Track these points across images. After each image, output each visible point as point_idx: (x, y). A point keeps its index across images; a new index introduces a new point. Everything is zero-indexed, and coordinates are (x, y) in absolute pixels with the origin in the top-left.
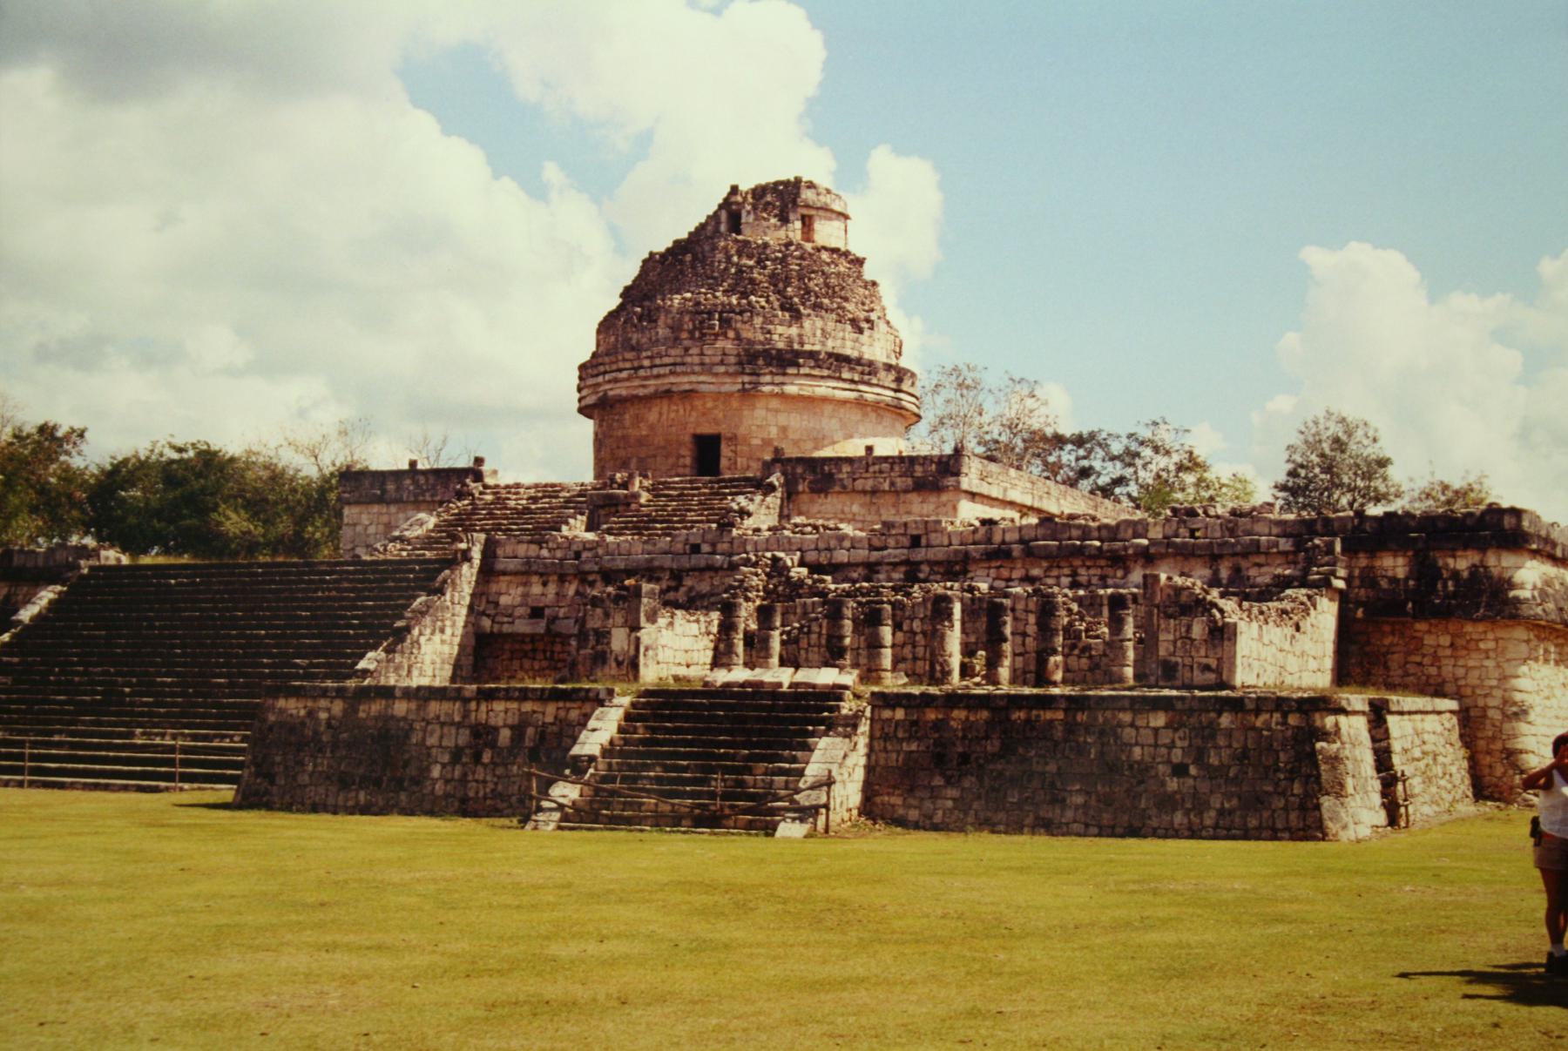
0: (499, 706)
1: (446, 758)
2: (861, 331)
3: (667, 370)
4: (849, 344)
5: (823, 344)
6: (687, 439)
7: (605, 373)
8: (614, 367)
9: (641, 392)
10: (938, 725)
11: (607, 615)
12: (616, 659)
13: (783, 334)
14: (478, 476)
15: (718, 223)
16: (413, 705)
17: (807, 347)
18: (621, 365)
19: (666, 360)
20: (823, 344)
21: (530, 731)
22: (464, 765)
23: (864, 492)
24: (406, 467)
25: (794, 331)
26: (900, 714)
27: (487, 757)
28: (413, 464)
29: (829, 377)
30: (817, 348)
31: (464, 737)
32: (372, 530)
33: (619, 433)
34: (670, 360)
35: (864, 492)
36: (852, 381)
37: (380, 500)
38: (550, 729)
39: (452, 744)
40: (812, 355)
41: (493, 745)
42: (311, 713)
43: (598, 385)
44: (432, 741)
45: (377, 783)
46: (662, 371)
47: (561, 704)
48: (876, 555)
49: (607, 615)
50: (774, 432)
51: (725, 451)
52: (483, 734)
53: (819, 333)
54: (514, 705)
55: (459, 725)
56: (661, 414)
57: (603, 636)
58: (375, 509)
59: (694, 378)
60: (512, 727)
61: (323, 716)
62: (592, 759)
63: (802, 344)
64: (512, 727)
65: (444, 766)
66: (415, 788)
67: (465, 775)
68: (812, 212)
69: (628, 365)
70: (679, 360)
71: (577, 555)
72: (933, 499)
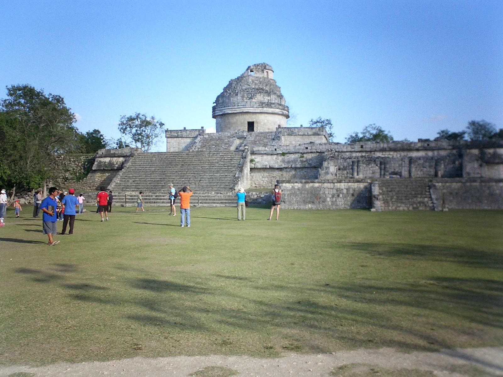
0: (342, 184)
1: (331, 196)
2: (281, 99)
4: (279, 101)
5: (275, 101)
6: (247, 123)
8: (227, 106)
9: (235, 112)
10: (450, 186)
11: (328, 163)
12: (331, 173)
13: (266, 99)
14: (203, 131)
15: (248, 73)
16: (320, 184)
17: (272, 102)
18: (229, 105)
20: (275, 101)
21: (351, 190)
22: (336, 198)
23: (301, 135)
24: (183, 129)
25: (269, 98)
26: (440, 184)
27: (341, 195)
28: (185, 128)
30: (274, 102)
31: (335, 191)
32: (175, 144)
34: (243, 104)
35: (301, 135)
37: (177, 137)
38: (356, 189)
39: (332, 193)
40: (274, 104)
41: (343, 194)
42: (293, 187)
43: (222, 110)
44: (327, 192)
45: (313, 202)
47: (358, 183)
48: (353, 150)
49: (328, 163)
50: (266, 121)
51: (255, 124)
52: (339, 190)
54: (346, 184)
55: (333, 189)
57: (327, 168)
58: (175, 139)
59: (248, 108)
60: (347, 189)
61: (296, 187)
62: (378, 195)
63: (271, 101)
64: (347, 189)
65: (330, 198)
66: (323, 203)
67: (336, 200)
70: (245, 104)
71: (276, 150)
72: (317, 137)
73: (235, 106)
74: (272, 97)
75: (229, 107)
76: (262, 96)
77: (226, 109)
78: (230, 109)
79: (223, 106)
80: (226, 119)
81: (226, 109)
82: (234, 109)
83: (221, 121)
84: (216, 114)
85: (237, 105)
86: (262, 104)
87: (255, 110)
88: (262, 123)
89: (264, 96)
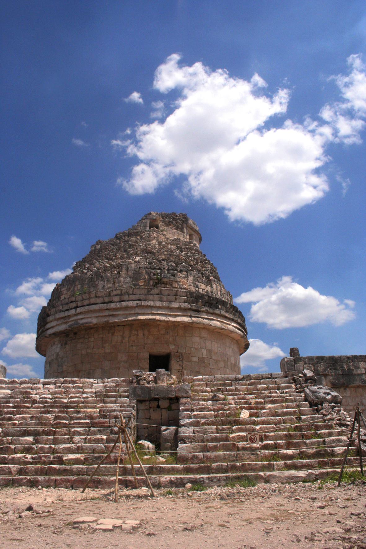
3: (135, 302)
6: (147, 355)
7: (76, 307)
8: (86, 302)
13: (203, 288)
18: (93, 300)
19: (133, 297)
25: (208, 289)
29: (232, 320)
33: (84, 352)
36: (239, 324)
43: (69, 317)
46: (131, 304)
50: (205, 352)
53: (219, 293)
56: (123, 337)
68: (193, 233)
69: (99, 300)
73: (111, 302)
74: (214, 286)
75: (92, 307)
76: (191, 278)
77: (81, 313)
78: (95, 311)
79: (74, 305)
80: (79, 346)
81: (81, 313)
82: (107, 313)
83: (61, 354)
84: (50, 332)
85: (117, 299)
86: (195, 297)
87: (176, 316)
88: (195, 359)
89: (195, 279)
